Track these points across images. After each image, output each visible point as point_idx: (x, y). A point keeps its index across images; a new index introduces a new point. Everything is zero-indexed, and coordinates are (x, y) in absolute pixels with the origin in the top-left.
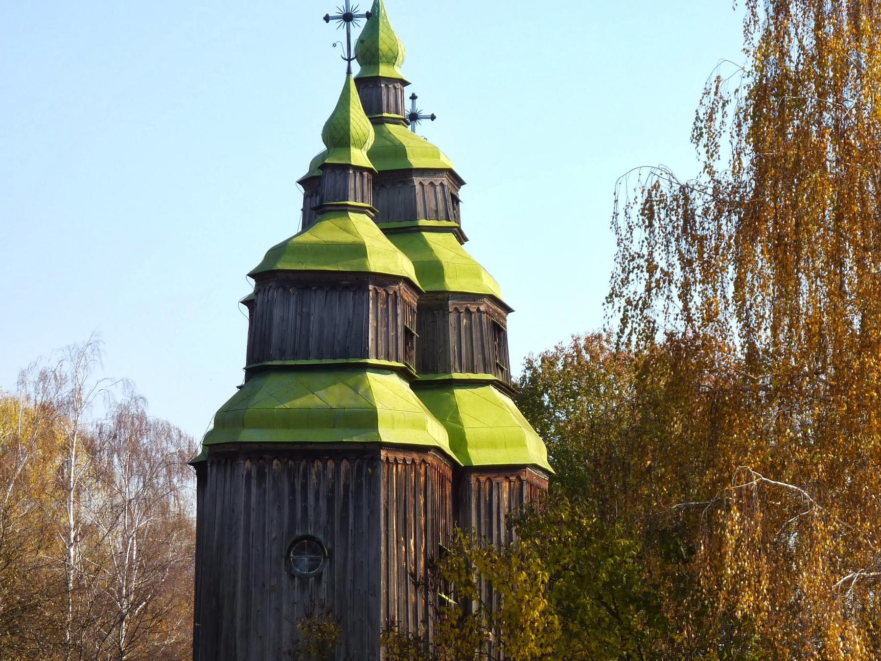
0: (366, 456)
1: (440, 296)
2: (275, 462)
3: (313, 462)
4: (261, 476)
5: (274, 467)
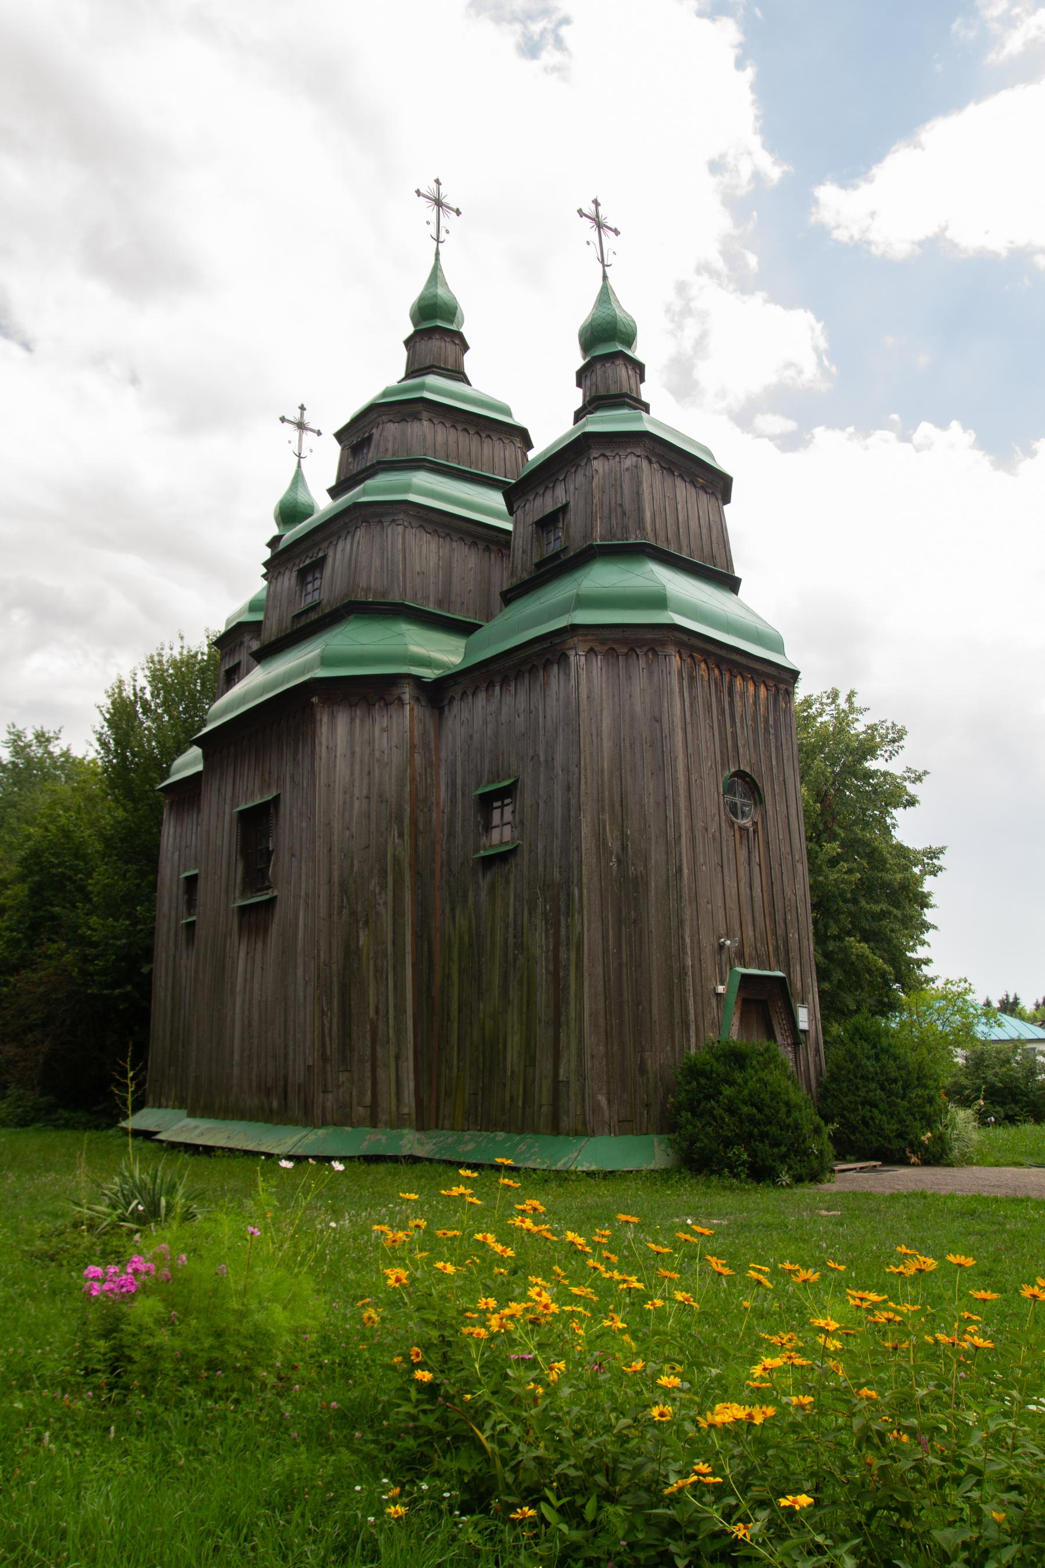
0: (781, 686)
5: (702, 672)
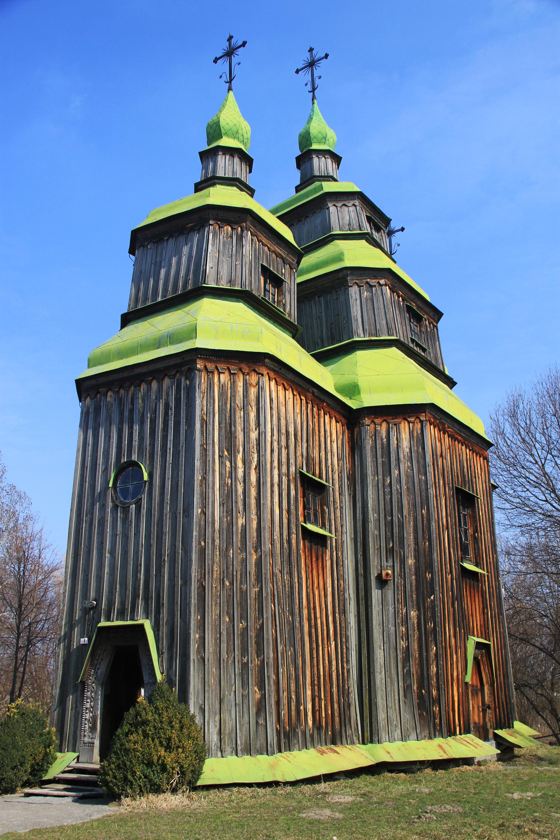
0: (183, 369)
1: (340, 275)
2: (110, 393)
3: (140, 386)
4: (97, 409)
5: (108, 399)
